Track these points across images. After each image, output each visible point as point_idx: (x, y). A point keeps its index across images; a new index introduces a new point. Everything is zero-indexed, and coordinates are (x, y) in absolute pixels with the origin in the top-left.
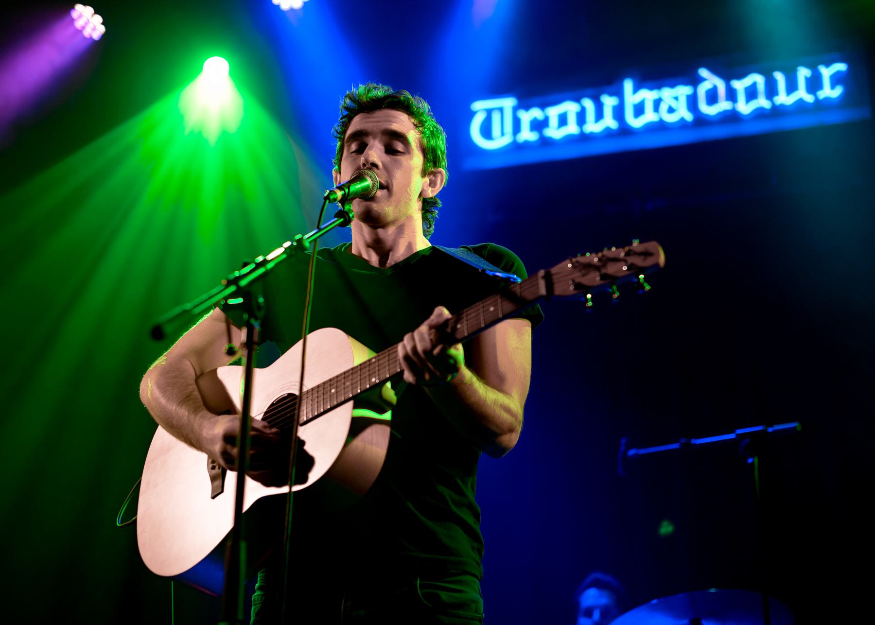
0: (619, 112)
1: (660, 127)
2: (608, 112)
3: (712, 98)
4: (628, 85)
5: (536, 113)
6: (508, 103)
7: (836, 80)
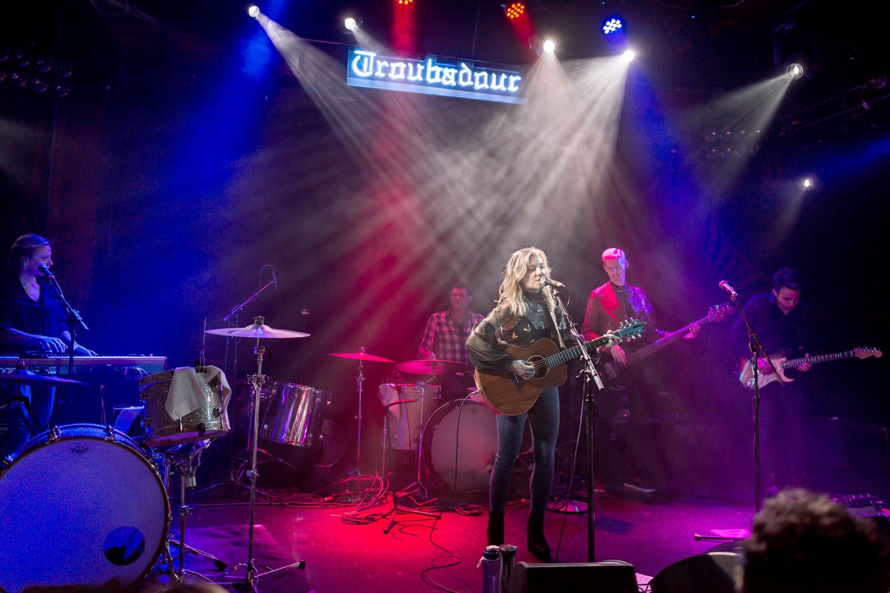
0: (424, 73)
1: (439, 85)
2: (419, 72)
3: (465, 78)
4: (430, 61)
5: (386, 64)
6: (373, 55)
7: (517, 83)
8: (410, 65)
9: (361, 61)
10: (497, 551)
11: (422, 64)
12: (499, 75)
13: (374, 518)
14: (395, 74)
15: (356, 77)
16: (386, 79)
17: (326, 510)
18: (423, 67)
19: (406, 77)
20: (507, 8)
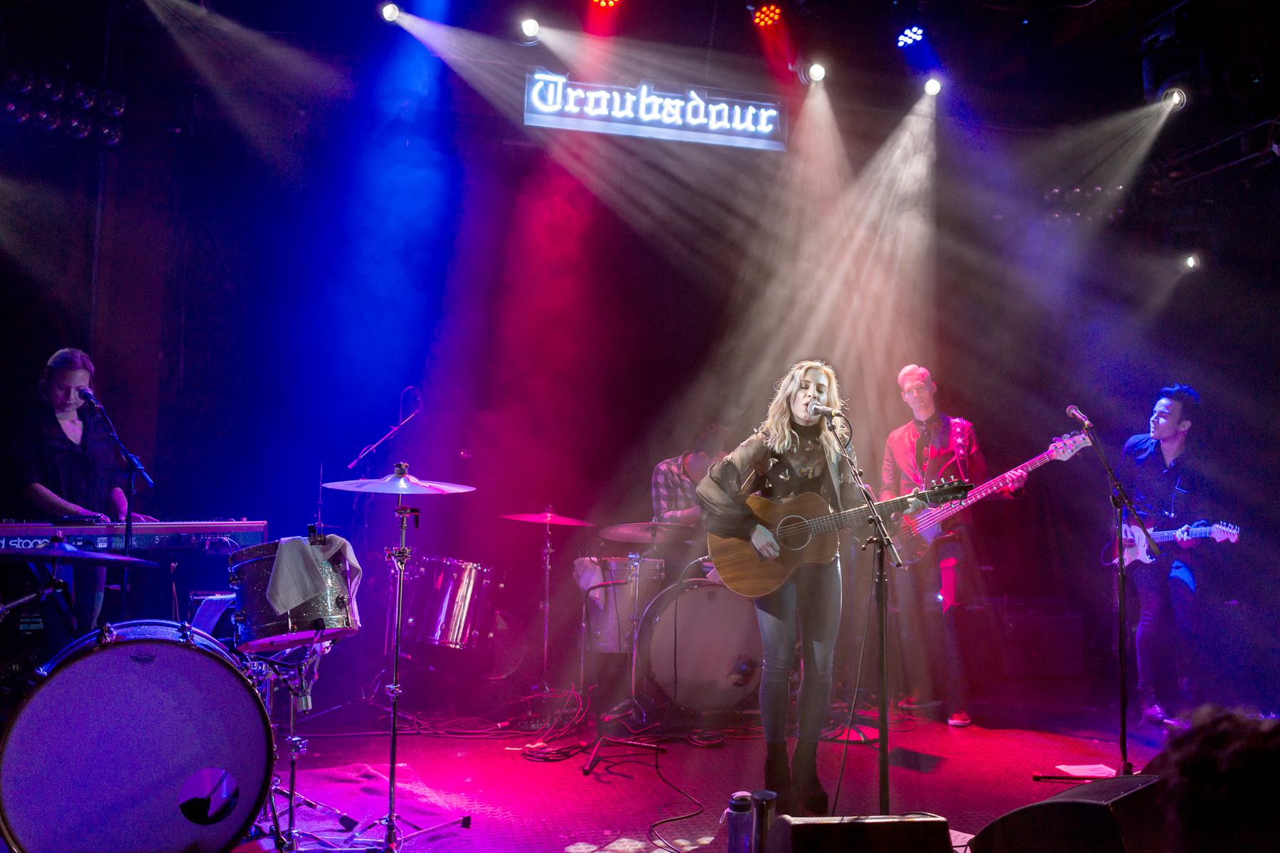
1: (658, 124)
2: (629, 105)
3: (695, 113)
4: (644, 89)
5: (580, 93)
8: (616, 95)
9: (544, 88)
10: (747, 800)
11: (632, 93)
12: (744, 108)
13: (569, 752)
14: (594, 108)
15: (537, 113)
16: (581, 115)
17: (499, 742)
18: (634, 98)
19: (610, 111)
20: (755, 11)
